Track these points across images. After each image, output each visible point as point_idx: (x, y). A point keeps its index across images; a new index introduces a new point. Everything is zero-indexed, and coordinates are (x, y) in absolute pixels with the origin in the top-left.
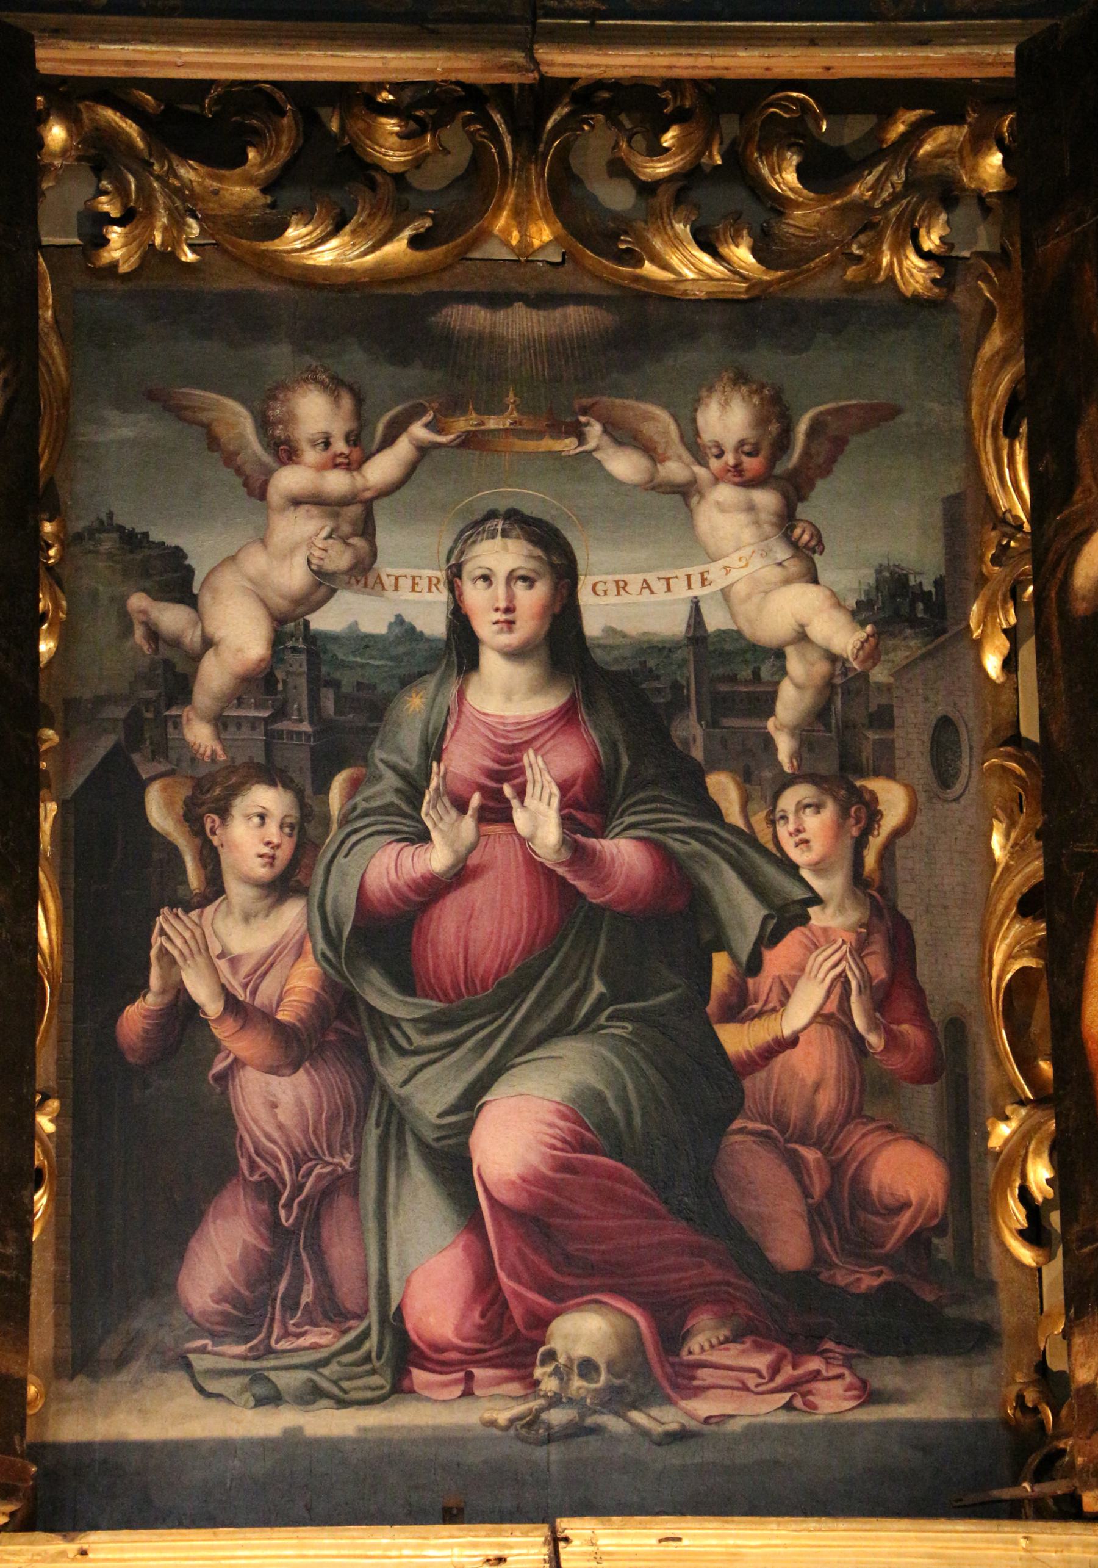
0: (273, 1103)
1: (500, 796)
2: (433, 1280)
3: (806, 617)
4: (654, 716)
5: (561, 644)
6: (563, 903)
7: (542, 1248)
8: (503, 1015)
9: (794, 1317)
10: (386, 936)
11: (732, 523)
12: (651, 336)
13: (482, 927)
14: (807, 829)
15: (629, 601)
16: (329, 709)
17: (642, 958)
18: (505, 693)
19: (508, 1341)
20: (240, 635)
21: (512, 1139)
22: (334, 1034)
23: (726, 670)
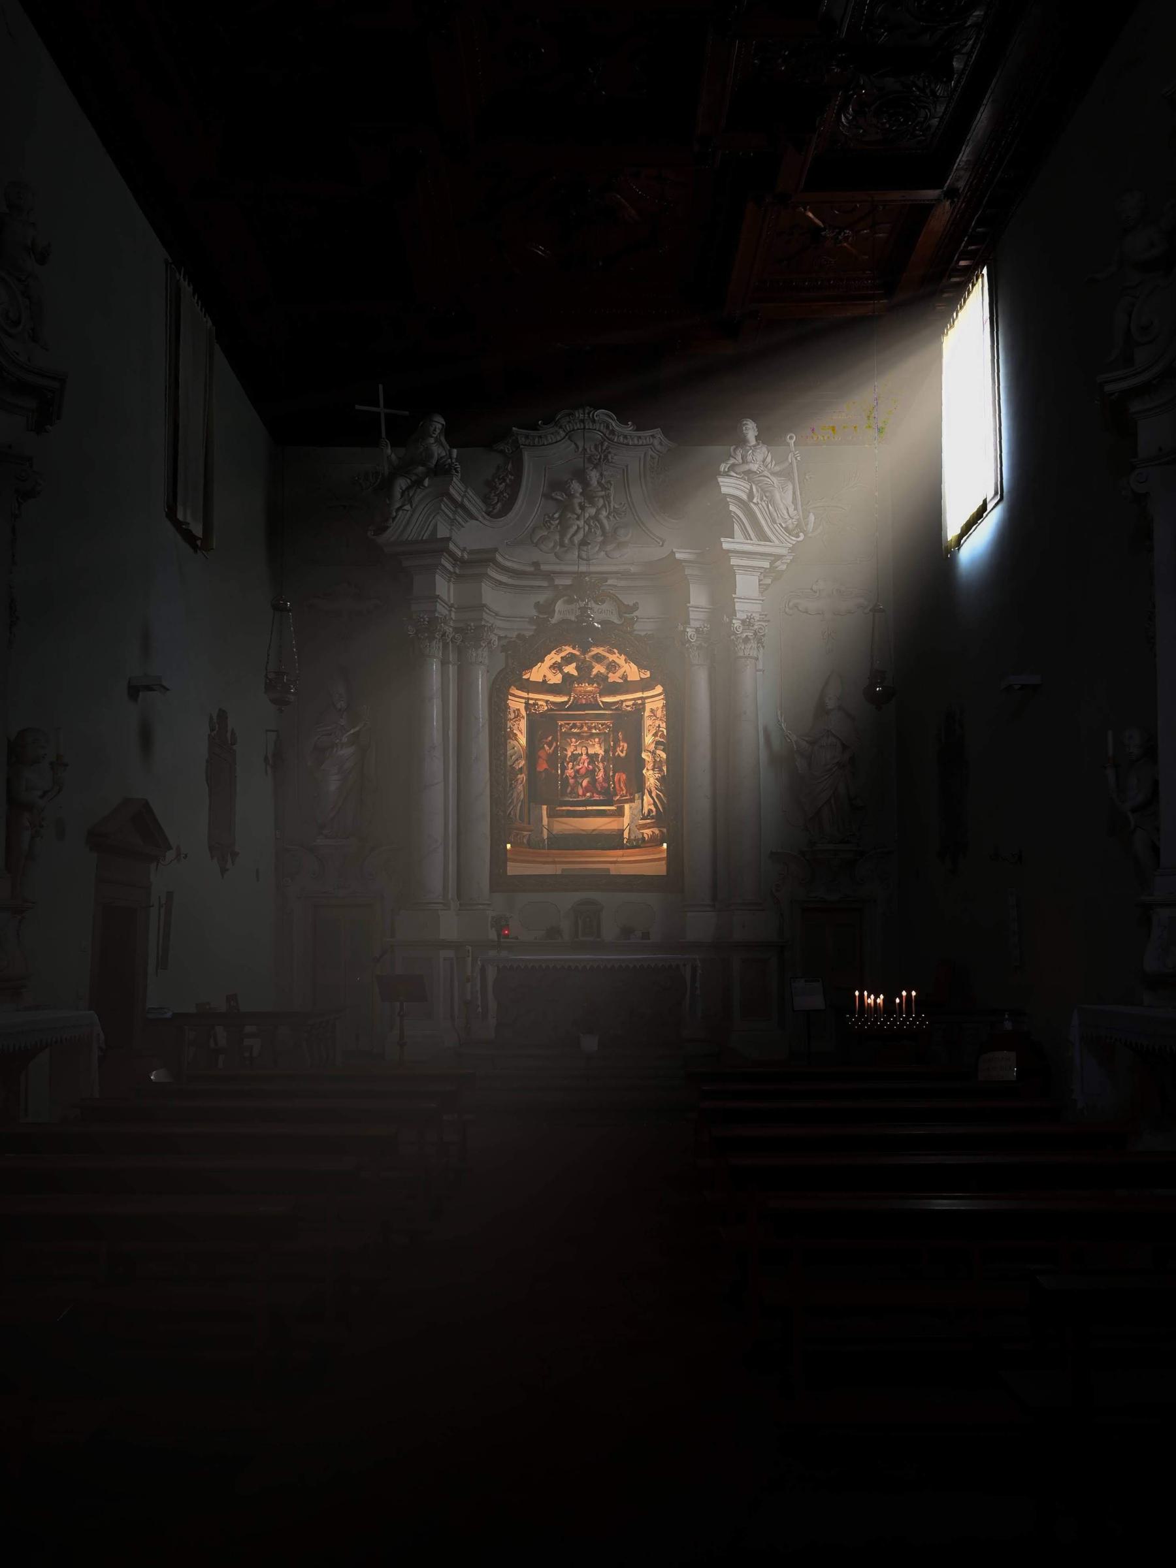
0: (571, 781)
1: (584, 764)
2: (581, 792)
3: (601, 752)
4: (593, 758)
5: (587, 754)
6: (587, 769)
7: (586, 790)
8: (584, 777)
9: (599, 793)
10: (578, 771)
11: (597, 746)
12: (592, 735)
13: (583, 771)
14: (601, 765)
15: (591, 751)
16: (575, 758)
17: (591, 773)
18: (584, 757)
19: (584, 795)
20: (569, 754)
21: (585, 783)
22: (575, 777)
23: (597, 755)
